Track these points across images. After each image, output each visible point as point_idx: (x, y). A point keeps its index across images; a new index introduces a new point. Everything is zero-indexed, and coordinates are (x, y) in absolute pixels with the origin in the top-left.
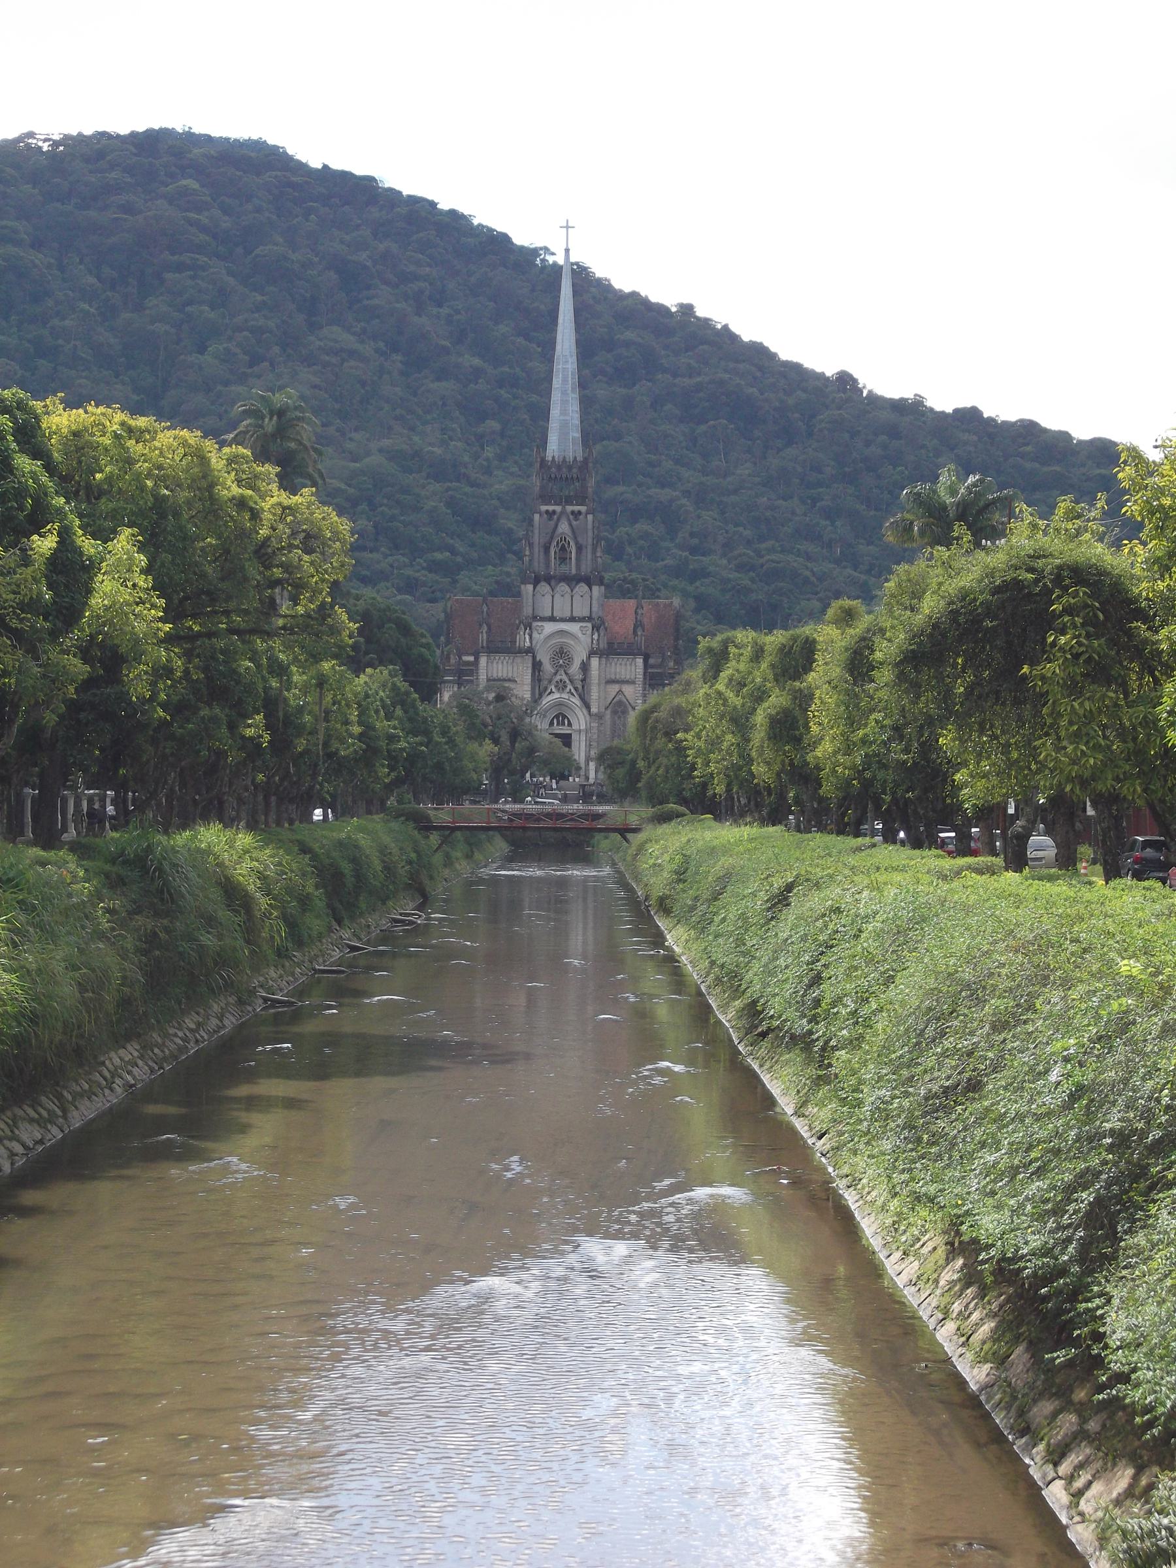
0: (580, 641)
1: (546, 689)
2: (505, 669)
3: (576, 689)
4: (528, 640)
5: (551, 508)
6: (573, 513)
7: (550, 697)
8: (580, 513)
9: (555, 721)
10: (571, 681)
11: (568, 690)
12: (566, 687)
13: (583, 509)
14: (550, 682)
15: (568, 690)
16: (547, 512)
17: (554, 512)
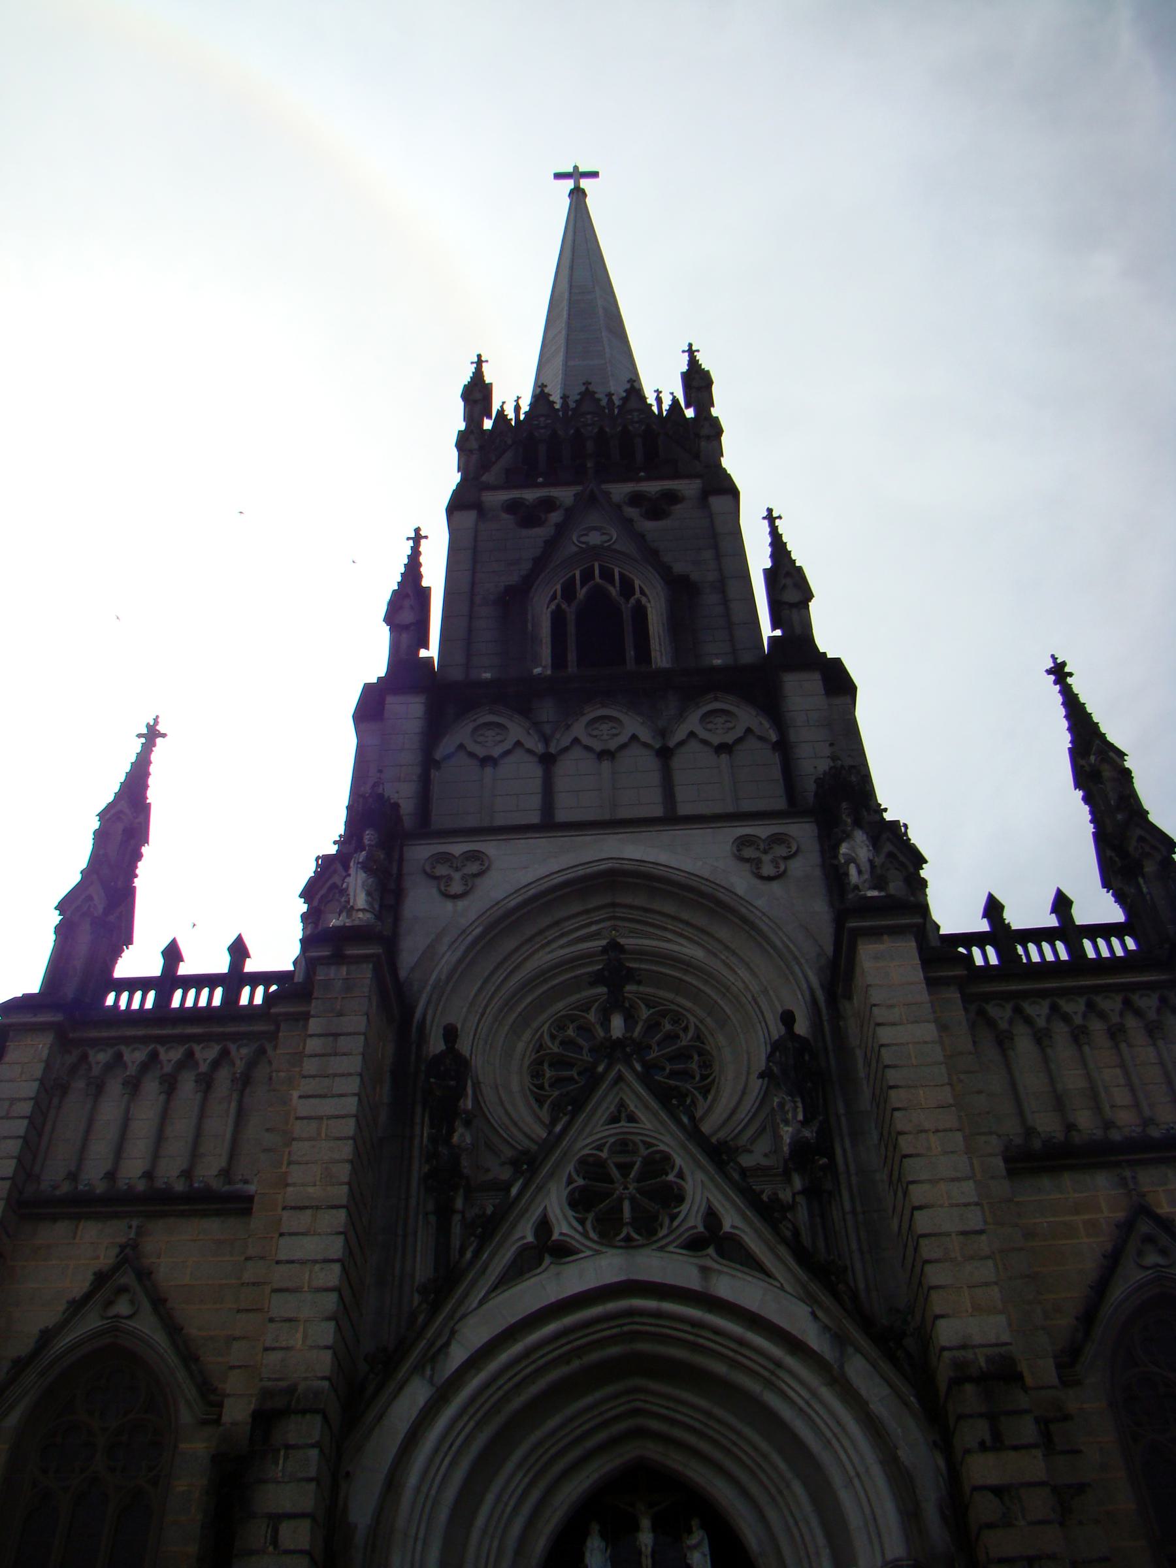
2: (181, 1126)
4: (360, 900)
5: (530, 495)
6: (636, 499)
8: (672, 498)
11: (691, 1217)
12: (673, 1197)
15: (691, 1217)
16: (513, 507)
17: (549, 504)
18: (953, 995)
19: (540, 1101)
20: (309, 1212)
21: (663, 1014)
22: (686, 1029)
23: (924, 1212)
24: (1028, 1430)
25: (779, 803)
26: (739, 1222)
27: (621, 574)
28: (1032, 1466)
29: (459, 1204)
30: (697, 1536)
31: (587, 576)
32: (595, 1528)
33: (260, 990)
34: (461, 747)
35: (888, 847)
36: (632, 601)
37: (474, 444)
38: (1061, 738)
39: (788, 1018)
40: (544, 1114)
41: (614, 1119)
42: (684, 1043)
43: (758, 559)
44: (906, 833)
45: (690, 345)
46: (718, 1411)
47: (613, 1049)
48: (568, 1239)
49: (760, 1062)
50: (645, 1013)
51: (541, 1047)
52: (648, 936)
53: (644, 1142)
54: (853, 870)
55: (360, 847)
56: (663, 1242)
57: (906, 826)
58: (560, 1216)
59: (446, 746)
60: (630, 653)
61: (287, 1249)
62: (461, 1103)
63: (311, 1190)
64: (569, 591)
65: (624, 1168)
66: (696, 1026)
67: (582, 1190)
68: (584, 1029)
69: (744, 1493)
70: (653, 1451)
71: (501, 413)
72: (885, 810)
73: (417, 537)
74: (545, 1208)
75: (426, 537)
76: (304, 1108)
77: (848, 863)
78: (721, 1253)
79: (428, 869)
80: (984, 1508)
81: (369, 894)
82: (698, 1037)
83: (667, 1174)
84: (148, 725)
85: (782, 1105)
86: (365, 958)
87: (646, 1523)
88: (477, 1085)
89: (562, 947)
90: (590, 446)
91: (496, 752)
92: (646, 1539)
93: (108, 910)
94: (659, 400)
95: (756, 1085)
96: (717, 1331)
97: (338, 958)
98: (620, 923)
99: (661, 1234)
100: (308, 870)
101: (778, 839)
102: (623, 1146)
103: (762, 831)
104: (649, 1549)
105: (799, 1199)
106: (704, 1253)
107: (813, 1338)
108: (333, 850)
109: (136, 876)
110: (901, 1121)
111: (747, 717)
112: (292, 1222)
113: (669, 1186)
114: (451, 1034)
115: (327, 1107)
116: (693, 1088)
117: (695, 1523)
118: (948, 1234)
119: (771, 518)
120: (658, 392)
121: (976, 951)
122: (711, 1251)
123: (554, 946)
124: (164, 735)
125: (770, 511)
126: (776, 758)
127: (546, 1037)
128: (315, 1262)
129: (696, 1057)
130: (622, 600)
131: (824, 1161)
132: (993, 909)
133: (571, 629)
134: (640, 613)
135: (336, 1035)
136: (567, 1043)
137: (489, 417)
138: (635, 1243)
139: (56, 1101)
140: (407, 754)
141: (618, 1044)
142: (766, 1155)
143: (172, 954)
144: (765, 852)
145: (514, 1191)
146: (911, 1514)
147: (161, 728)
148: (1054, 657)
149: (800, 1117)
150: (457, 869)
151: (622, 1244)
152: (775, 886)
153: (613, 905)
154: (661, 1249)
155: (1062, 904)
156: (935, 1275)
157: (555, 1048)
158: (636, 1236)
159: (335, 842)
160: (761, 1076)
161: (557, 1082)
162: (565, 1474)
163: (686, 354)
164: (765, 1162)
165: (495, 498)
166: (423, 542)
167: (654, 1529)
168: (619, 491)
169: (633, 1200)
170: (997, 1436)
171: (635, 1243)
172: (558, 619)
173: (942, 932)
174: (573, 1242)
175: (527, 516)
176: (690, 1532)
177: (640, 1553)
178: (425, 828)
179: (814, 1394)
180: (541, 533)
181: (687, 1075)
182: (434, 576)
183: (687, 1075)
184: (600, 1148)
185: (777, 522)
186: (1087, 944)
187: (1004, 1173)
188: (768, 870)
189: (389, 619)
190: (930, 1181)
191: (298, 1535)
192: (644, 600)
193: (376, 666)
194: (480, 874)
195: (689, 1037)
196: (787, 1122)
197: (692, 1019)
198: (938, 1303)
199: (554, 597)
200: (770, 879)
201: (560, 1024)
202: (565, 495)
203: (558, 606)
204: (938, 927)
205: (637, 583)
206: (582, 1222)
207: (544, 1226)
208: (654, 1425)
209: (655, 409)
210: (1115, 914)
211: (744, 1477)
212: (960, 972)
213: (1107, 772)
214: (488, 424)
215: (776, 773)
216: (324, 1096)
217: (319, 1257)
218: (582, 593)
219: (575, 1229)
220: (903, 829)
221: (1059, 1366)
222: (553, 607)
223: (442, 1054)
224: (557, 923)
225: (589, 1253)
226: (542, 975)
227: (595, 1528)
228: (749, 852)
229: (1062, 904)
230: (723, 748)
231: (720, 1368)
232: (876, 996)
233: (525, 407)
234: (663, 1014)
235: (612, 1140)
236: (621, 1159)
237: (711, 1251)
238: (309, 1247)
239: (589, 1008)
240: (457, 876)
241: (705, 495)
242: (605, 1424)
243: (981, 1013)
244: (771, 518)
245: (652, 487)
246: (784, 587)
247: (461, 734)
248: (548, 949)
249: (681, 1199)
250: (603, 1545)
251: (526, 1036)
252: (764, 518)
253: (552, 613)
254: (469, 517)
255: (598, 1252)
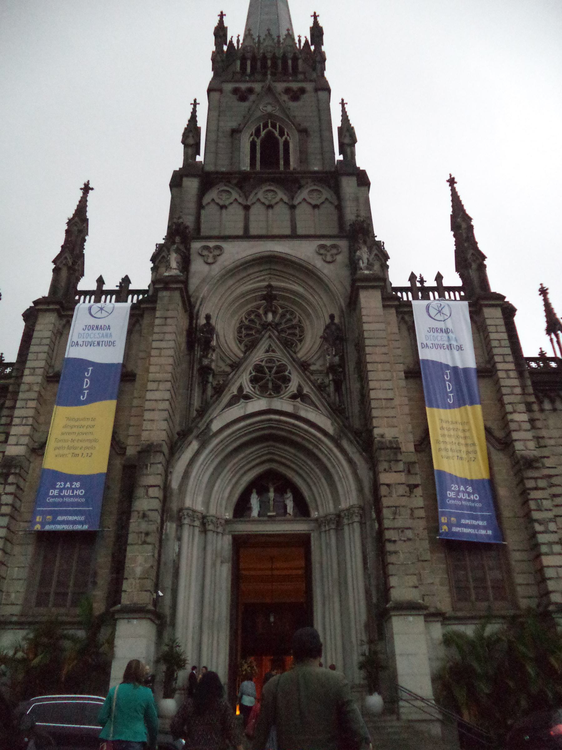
0: (319, 280)
1: (219, 391)
3: (321, 388)
4: (174, 264)
5: (243, 86)
6: (288, 91)
7: (236, 412)
9: (255, 501)
10: (304, 366)
11: (293, 387)
12: (286, 380)
13: (309, 86)
14: (235, 366)
15: (293, 387)
17: (251, 91)
18: (393, 311)
19: (240, 342)
20: (156, 383)
21: (287, 311)
22: (295, 317)
23: (373, 391)
24: (401, 466)
25: (335, 231)
26: (309, 390)
27: (280, 126)
28: (402, 478)
29: (211, 379)
30: (289, 495)
31: (265, 126)
32: (254, 491)
33: (135, 297)
34: (213, 200)
35: (375, 252)
36: (284, 138)
37: (219, 58)
38: (449, 210)
39: (332, 317)
40: (242, 347)
41: (267, 351)
42: (294, 323)
43: (336, 122)
44: (383, 246)
45: (315, 13)
46: (298, 454)
47: (266, 326)
48: (249, 394)
49: (321, 333)
50: (280, 311)
51: (242, 321)
52: (283, 282)
53: (277, 360)
54: (361, 262)
55: (174, 243)
56: (282, 397)
57: (383, 243)
58: (246, 386)
59: (207, 199)
60: (282, 162)
61: (149, 396)
62: (212, 343)
63: (158, 375)
64: (258, 132)
65: (270, 369)
66: (299, 317)
67: (255, 376)
68: (258, 316)
69: (305, 480)
70: (274, 466)
71: (231, 42)
72: (376, 236)
73: (195, 104)
74: (241, 383)
75: (199, 104)
76: (155, 345)
77: (359, 260)
78: (302, 400)
79: (200, 252)
80: (383, 490)
81: (177, 263)
82: (300, 321)
83: (285, 372)
84: (85, 184)
85: (327, 349)
86: (176, 289)
87: (272, 490)
88: (217, 336)
89: (251, 284)
90: (269, 62)
91: (227, 203)
92: (272, 495)
93: (74, 263)
94: (300, 41)
95: (319, 341)
96: (299, 427)
97: (166, 289)
98: (272, 276)
99: (282, 393)
100: (152, 250)
101: (334, 246)
102: (270, 360)
103: (328, 243)
104: (273, 498)
105: (331, 382)
106: (297, 400)
107: (331, 431)
108: (163, 242)
109: (84, 249)
110: (369, 358)
111: (326, 194)
112: (151, 386)
113: (285, 376)
114: (208, 317)
115: (163, 345)
116: (298, 340)
117: (288, 490)
118: (381, 399)
119: (343, 104)
120: (299, 37)
121: (404, 294)
122: (299, 400)
123: (247, 284)
124: (92, 189)
125: (343, 100)
126: (335, 212)
127: (244, 319)
128: (160, 400)
129: (298, 328)
130: (279, 137)
131: (341, 370)
132: (412, 277)
133: (258, 148)
134: (286, 143)
135: (166, 318)
136: (251, 321)
137: (226, 44)
138: (272, 396)
139: (58, 338)
140: (191, 205)
141: (270, 324)
142: (321, 366)
143: (100, 281)
144: (328, 251)
145: (230, 376)
146: (360, 490)
147: (91, 186)
148: (450, 175)
149: (334, 353)
150: (211, 252)
151: (268, 396)
152: (331, 266)
153: (270, 269)
154: (282, 398)
155: (439, 278)
156: (375, 413)
157: (247, 323)
158: (273, 393)
159: (164, 239)
160: (321, 337)
161: (247, 335)
162: (245, 473)
163: (313, 18)
164: (320, 368)
165: (229, 87)
166: (197, 106)
167: (275, 491)
168: (280, 86)
169: (272, 380)
170: (390, 468)
171: (272, 396)
172: (253, 145)
173: (393, 286)
174: (250, 395)
175: (242, 95)
176: (286, 493)
177: (269, 499)
178: (198, 235)
179: (331, 450)
180: (246, 104)
181: (294, 334)
182: (202, 122)
183: (294, 334)
184: (262, 361)
185: (346, 106)
186: (446, 293)
187: (404, 378)
188: (329, 258)
189: (183, 142)
190: (376, 380)
191: (155, 492)
192: (288, 138)
193: (178, 164)
194: (219, 255)
195: (296, 321)
196: (329, 355)
197: (297, 314)
198: (375, 422)
199: (251, 135)
200: (329, 262)
201: (249, 314)
202: (257, 87)
203: (253, 139)
204: (391, 284)
205: (286, 130)
206: (254, 388)
207: (241, 389)
208: (276, 458)
209: (298, 45)
210: (458, 282)
211: (305, 475)
212: (396, 303)
213: (464, 226)
214: (225, 48)
215: (335, 218)
216: (162, 341)
217: (161, 399)
218: (263, 133)
219: (252, 391)
220: (382, 244)
221: (415, 446)
222: (251, 139)
223: (204, 325)
224: (249, 275)
225: (256, 399)
226: (243, 295)
227: (254, 491)
228: (322, 251)
229: (439, 278)
230: (315, 207)
231: (299, 440)
232: (364, 312)
233: (241, 41)
234: (287, 311)
235: (266, 359)
236: (270, 365)
237: (299, 400)
238: (157, 395)
239: (260, 308)
240: (211, 255)
241: (316, 90)
242: (259, 457)
243: (403, 318)
244: (343, 104)
245: (295, 86)
246: (345, 136)
247: (213, 194)
248: (245, 285)
249: (289, 380)
250: (257, 496)
251: (236, 318)
252: (340, 103)
253: (251, 142)
254: (216, 95)
255: (259, 399)
